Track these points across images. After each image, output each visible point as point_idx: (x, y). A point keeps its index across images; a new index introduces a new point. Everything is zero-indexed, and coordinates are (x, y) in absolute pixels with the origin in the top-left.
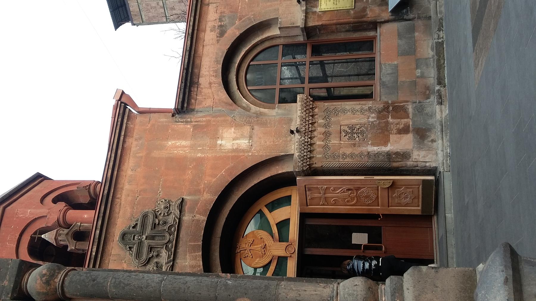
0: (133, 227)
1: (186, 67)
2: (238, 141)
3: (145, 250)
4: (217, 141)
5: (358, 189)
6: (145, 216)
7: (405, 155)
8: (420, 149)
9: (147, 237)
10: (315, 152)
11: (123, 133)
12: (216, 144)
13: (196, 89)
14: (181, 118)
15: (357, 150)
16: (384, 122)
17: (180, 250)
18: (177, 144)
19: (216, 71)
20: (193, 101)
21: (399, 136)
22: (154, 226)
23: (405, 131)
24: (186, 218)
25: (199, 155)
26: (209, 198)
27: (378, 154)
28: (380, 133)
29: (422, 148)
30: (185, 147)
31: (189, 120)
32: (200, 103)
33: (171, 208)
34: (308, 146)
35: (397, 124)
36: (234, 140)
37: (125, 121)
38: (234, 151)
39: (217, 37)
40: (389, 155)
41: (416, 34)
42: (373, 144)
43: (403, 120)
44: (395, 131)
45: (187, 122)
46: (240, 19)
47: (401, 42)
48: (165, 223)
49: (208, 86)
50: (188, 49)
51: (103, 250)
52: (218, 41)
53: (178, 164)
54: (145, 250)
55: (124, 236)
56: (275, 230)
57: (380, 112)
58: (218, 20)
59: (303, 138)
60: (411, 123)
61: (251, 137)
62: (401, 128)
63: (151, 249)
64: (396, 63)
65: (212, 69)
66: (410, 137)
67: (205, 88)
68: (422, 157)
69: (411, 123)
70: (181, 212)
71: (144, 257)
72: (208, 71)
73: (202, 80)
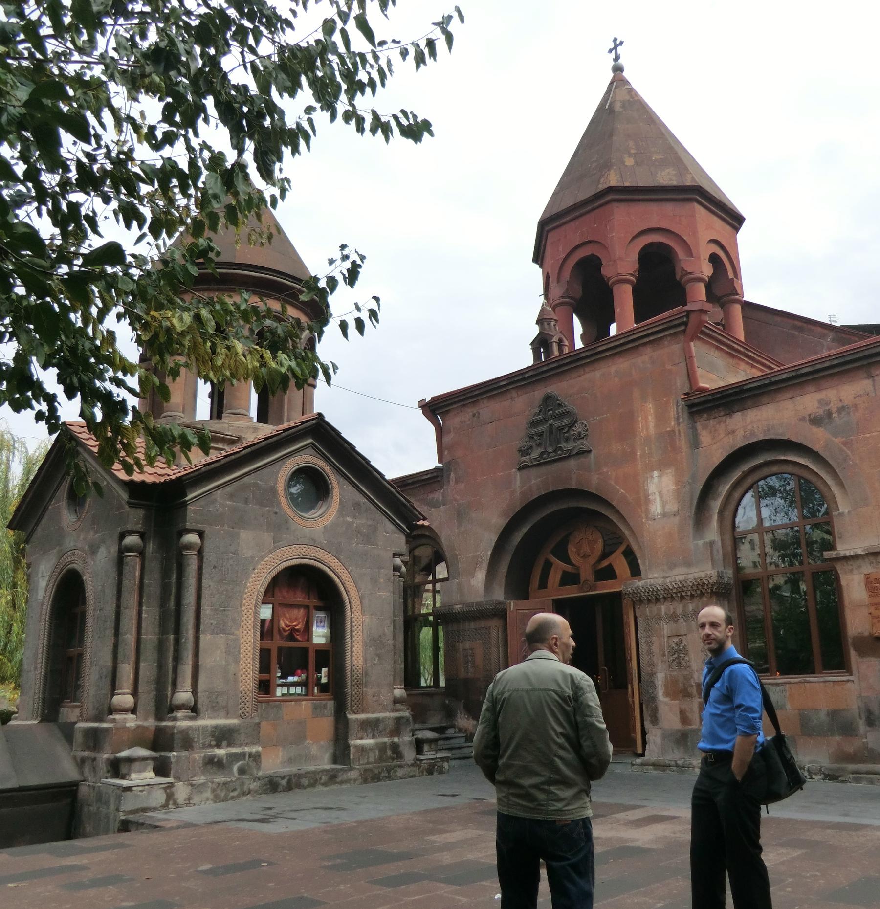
0: (560, 405)
1: (745, 388)
2: (658, 499)
3: (541, 428)
4: (656, 469)
6: (567, 414)
7: (655, 720)
8: (664, 737)
9: (551, 425)
10: (651, 605)
11: (652, 338)
12: (652, 471)
13: (722, 413)
14: (682, 410)
15: (656, 659)
17: (543, 470)
18: (650, 418)
19: (753, 433)
20: (705, 415)
22: (560, 429)
23: (684, 718)
24: (572, 463)
25: (639, 452)
26: (593, 483)
27: (653, 685)
30: (647, 429)
31: (681, 420)
32: (705, 427)
33: (580, 441)
34: (654, 598)
36: (660, 493)
37: (667, 333)
38: (647, 496)
39: (809, 415)
40: (654, 699)
41: (838, 738)
42: (666, 677)
45: (678, 418)
46: (845, 444)
47: (823, 716)
48: (567, 440)
49: (730, 428)
50: (773, 380)
51: (534, 382)
52: (802, 419)
53: (627, 428)
54: (541, 428)
55: (548, 398)
56: (605, 563)
58: (840, 405)
59: (659, 588)
61: (664, 515)
63: (540, 435)
64: (788, 706)
65: (755, 426)
67: (726, 426)
69: (694, 727)
70: (577, 454)
71: (533, 431)
72: (752, 422)
73: (738, 416)
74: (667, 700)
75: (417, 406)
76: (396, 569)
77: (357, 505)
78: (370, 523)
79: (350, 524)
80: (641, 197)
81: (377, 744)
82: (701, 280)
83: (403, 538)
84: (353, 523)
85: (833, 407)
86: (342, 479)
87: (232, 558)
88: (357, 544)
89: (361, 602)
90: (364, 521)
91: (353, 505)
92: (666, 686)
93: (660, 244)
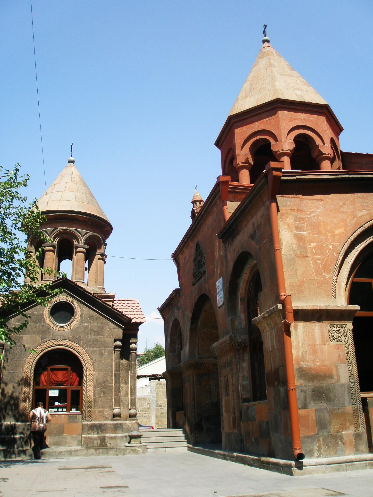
75: (171, 256)
76: (115, 347)
77: (91, 317)
78: (100, 325)
79: (87, 327)
80: (247, 116)
81: (99, 437)
82: (285, 154)
83: (121, 331)
84: (88, 326)
85: (256, 226)
86: (82, 305)
87: (19, 348)
88: (91, 336)
89: (93, 365)
90: (96, 324)
91: (89, 317)
93: (261, 138)
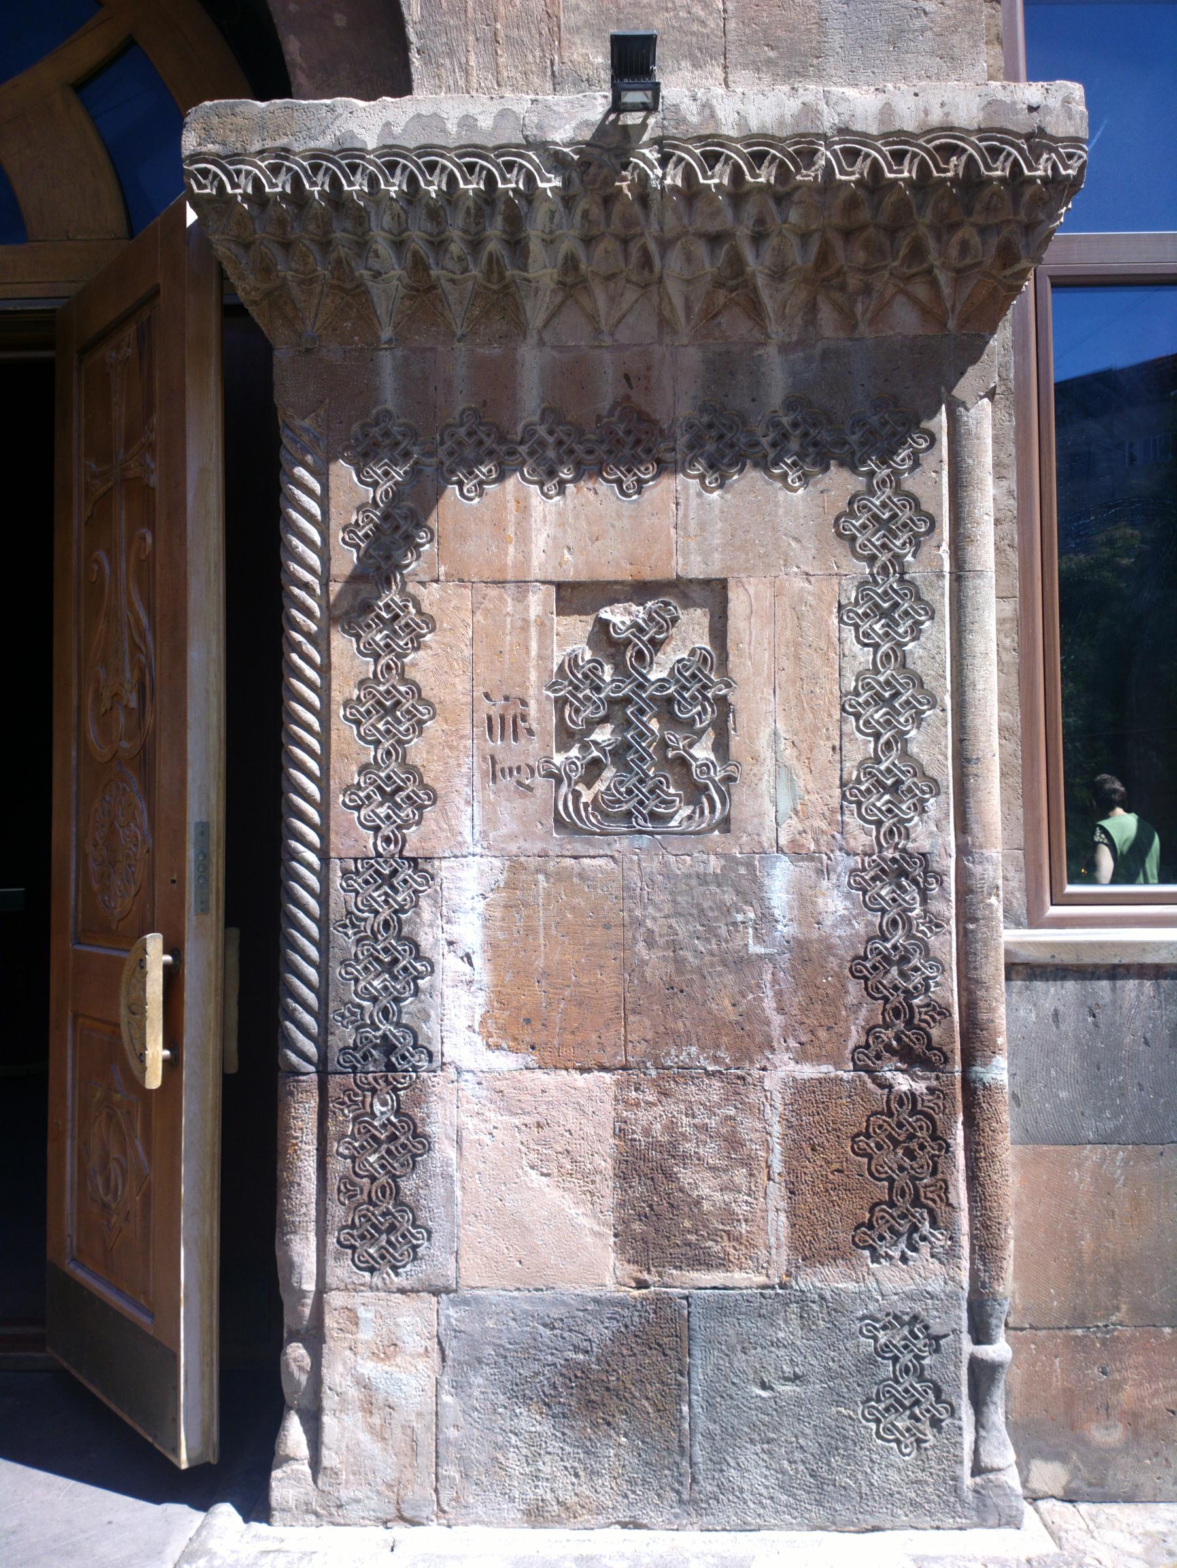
5: (144, 762)
16: (753, 1015)
21: (607, 1165)
23: (655, 1210)
28: (631, 968)
29: (458, 1388)
35: (733, 1142)
40: (395, 1057)
43: (776, 1193)
44: (652, 1119)
57: (869, 967)
60: (738, 1277)
62: (686, 1176)
66: (593, 1264)
68: (365, 1385)
69: (738, 1277)
74: (505, 1062)
92: (508, 952)
